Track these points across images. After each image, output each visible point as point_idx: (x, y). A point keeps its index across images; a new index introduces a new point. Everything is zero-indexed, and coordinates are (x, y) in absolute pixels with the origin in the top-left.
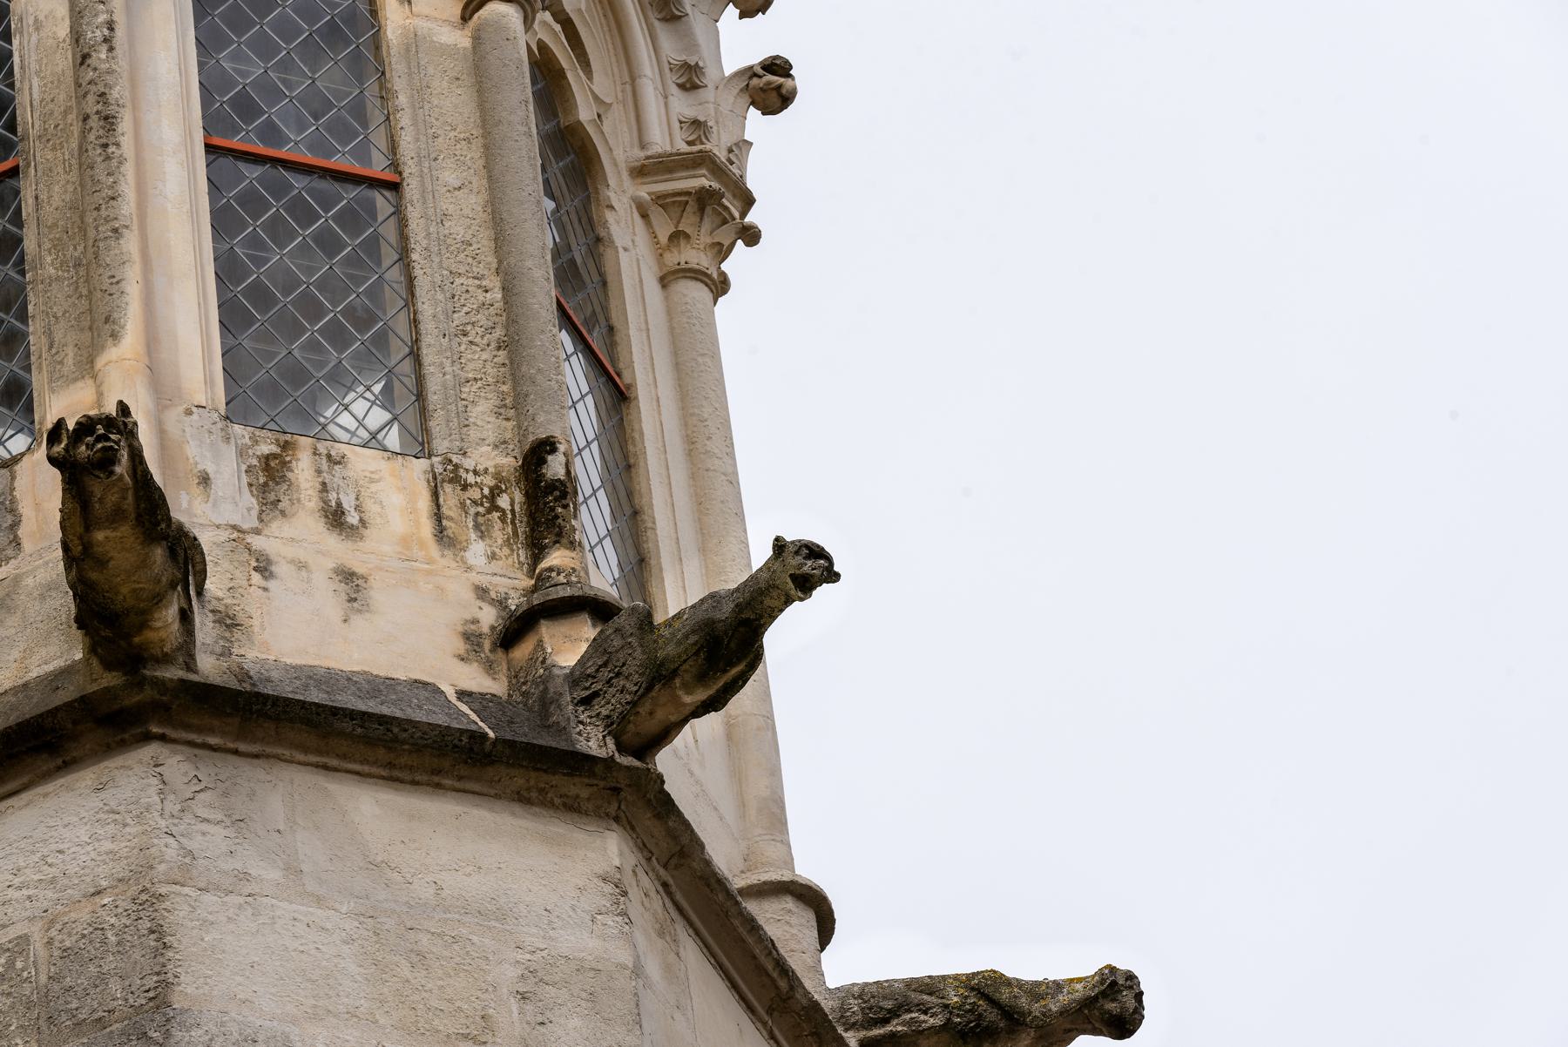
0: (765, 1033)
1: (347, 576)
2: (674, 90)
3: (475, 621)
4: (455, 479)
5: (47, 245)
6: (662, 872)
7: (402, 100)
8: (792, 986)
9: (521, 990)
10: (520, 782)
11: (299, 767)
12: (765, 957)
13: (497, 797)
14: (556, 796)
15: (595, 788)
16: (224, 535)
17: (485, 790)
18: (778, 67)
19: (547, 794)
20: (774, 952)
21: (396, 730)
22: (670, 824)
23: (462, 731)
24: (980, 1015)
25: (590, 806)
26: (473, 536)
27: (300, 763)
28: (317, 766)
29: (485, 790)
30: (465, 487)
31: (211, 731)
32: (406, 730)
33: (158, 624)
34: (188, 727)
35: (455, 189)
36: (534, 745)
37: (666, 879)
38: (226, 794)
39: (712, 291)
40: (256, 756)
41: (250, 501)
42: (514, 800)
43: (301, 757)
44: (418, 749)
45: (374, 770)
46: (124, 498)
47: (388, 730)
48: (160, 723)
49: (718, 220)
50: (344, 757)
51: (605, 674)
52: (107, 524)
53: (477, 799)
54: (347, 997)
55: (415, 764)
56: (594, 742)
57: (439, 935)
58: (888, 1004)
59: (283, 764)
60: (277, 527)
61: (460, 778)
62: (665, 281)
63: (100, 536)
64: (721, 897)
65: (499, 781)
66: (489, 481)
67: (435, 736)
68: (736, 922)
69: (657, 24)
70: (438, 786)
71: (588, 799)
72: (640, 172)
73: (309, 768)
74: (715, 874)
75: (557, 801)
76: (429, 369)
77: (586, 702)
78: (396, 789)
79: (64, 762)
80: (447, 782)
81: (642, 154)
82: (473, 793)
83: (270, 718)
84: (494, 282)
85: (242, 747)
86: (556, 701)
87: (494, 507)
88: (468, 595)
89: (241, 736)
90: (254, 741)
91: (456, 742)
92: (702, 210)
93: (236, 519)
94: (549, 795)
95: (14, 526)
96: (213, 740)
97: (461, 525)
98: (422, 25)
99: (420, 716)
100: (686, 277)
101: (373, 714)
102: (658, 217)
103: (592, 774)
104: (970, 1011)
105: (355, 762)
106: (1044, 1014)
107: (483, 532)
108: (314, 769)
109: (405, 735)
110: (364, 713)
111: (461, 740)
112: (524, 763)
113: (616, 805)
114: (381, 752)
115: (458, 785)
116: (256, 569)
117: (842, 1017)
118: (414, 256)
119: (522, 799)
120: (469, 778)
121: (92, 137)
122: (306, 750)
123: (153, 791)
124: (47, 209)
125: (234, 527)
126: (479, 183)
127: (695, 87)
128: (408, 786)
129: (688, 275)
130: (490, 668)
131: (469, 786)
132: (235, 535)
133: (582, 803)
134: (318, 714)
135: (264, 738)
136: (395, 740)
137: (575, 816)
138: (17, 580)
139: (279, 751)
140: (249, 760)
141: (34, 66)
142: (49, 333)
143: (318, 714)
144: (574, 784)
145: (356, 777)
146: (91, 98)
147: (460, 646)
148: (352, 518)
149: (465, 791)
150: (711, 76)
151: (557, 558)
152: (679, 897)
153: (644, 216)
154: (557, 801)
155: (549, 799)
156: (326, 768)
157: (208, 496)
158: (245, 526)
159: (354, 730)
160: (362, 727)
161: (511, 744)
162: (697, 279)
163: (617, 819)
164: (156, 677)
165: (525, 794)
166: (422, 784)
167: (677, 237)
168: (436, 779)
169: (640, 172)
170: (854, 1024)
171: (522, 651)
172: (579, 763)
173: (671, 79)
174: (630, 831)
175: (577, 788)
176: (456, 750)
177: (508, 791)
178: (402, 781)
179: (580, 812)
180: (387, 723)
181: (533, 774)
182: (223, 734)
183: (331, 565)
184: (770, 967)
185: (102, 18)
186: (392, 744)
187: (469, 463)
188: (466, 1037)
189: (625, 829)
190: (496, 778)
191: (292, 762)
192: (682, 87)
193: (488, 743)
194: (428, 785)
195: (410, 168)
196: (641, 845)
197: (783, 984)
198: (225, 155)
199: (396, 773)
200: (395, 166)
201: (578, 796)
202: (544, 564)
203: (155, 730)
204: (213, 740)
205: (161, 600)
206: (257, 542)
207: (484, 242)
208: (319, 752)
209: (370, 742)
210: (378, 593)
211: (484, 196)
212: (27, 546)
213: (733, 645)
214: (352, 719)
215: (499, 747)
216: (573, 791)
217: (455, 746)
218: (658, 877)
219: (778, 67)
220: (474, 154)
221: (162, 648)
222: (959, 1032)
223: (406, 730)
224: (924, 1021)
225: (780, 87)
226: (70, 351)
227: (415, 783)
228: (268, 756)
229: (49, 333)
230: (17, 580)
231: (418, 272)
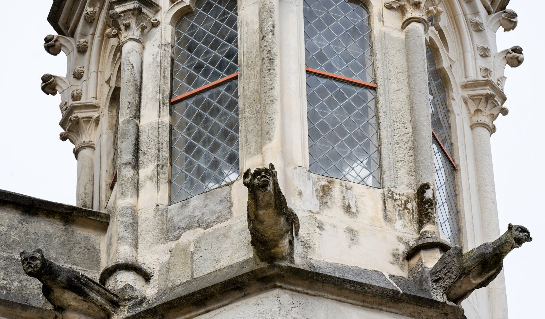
1: (351, 231)
2: (479, 57)
3: (397, 250)
4: (392, 197)
5: (247, 105)
7: (379, 57)
10: (411, 309)
11: (330, 300)
13: (402, 314)
15: (439, 313)
16: (307, 214)
17: (398, 312)
18: (517, 50)
19: (421, 314)
21: (366, 288)
23: (390, 290)
26: (398, 218)
27: (330, 299)
28: (337, 300)
29: (398, 312)
30: (395, 200)
31: (299, 285)
32: (370, 289)
33: (281, 246)
34: (290, 284)
35: (397, 90)
36: (417, 296)
38: (303, 309)
39: (489, 132)
40: (315, 296)
41: (317, 202)
42: (408, 316)
44: (374, 296)
45: (358, 303)
46: (271, 199)
47: (363, 288)
48: (280, 282)
49: (493, 106)
50: (347, 297)
51: (444, 271)
52: (264, 208)
53: (395, 315)
56: (439, 296)
59: (324, 299)
60: (326, 212)
61: (389, 307)
62: (472, 127)
63: (261, 212)
65: (403, 309)
66: (404, 198)
67: (381, 291)
69: (474, 33)
70: (381, 310)
71: (436, 317)
72: (465, 87)
73: (334, 301)
76: (384, 156)
77: (437, 281)
78: (365, 310)
79: (244, 294)
80: (384, 308)
81: (466, 80)
82: (394, 313)
83: (320, 282)
84: (409, 125)
85: (310, 292)
86: (425, 280)
87: (406, 208)
88: (395, 240)
89: (309, 288)
90: (314, 290)
92: (487, 102)
93: (311, 208)
94: (421, 315)
95: (230, 207)
96: (299, 289)
97: (393, 214)
98: (387, 30)
99: (375, 284)
100: (480, 126)
101: (358, 282)
102: (470, 102)
105: (351, 299)
107: (401, 217)
109: (369, 290)
110: (355, 282)
111: (390, 293)
112: (413, 303)
114: (360, 296)
115: (388, 309)
116: (317, 227)
118: (380, 114)
120: (392, 307)
121: (265, 66)
122: (333, 294)
123: (277, 306)
124: (248, 92)
125: (310, 211)
126: (406, 89)
127: (486, 56)
128: (370, 309)
129: (481, 125)
130: (402, 267)
132: (311, 214)
134: (338, 281)
135: (318, 289)
136: (366, 292)
138: (230, 227)
139: (323, 294)
140: (312, 297)
141: (245, 40)
142: (246, 137)
143: (338, 281)
144: (431, 311)
145: (351, 305)
146: (265, 52)
147: (391, 259)
148: (354, 210)
149: (391, 312)
150: (492, 53)
151: (428, 227)
153: (466, 103)
155: (421, 316)
156: (340, 301)
157: (301, 199)
158: (314, 211)
159: (351, 288)
160: (354, 287)
161: (408, 295)
162: (484, 127)
164: (280, 265)
166: (375, 309)
167: (477, 111)
168: (380, 307)
169: (465, 87)
171: (414, 261)
172: (433, 304)
173: (478, 53)
176: (388, 296)
177: (406, 313)
178: (368, 307)
180: (363, 286)
181: (416, 307)
182: (303, 287)
185: (271, 23)
186: (365, 293)
187: (397, 191)
190: (403, 308)
191: (328, 298)
192: (482, 56)
193: (400, 295)
194: (377, 309)
195: (380, 82)
199: (366, 304)
200: (375, 81)
201: (432, 316)
202: (423, 230)
203: (278, 284)
204: (299, 289)
205: (282, 237)
206: (318, 217)
207: (406, 110)
208: (338, 295)
209: (356, 292)
210: (362, 237)
211: (407, 93)
212: (235, 214)
214: (351, 284)
215: (404, 296)
217: (388, 295)
219: (517, 50)
220: (404, 78)
221: (282, 254)
223: (370, 289)
225: (518, 57)
226: (253, 144)
227: (372, 308)
228: (319, 296)
229: (246, 137)
230: (230, 227)
231: (381, 120)
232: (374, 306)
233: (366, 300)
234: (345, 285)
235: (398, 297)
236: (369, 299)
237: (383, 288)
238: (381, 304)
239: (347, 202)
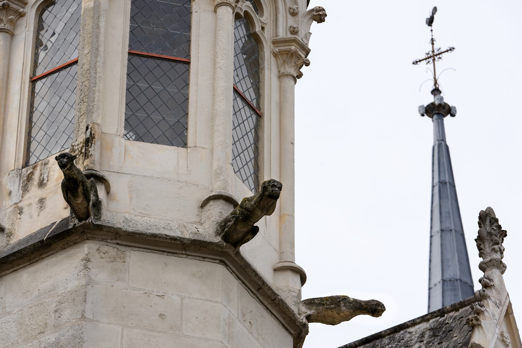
0: (185, 256)
6: (114, 241)
8: (181, 241)
9: (55, 310)
10: (61, 244)
12: (166, 240)
13: (57, 252)
14: (71, 243)
19: (68, 243)
20: (168, 237)
21: (23, 252)
22: (104, 230)
23: (38, 242)
24: (244, 213)
25: (80, 240)
27: (9, 273)
28: (13, 272)
29: (54, 252)
32: (25, 251)
35: (87, 54)
36: (55, 235)
37: (116, 242)
39: (228, 6)
42: (62, 250)
43: (8, 272)
44: (32, 253)
45: (26, 264)
47: (21, 253)
50: (19, 265)
54: (12, 339)
55: (35, 256)
57: (37, 305)
58: (223, 224)
60: (28, 195)
61: (47, 253)
64: (137, 236)
65: (56, 247)
67: (33, 247)
68: (149, 238)
70: (42, 258)
73: (11, 273)
74: (130, 232)
75: (72, 244)
78: (33, 266)
80: (44, 256)
82: (51, 255)
91: (38, 246)
100: (218, 7)
101: (16, 252)
103: (73, 233)
104: (242, 213)
105: (21, 264)
106: (251, 206)
108: (13, 273)
109: (26, 252)
110: (14, 253)
111: (39, 245)
112: (56, 241)
113: (86, 235)
115: (46, 255)
117: (217, 233)
119: (63, 249)
120: (49, 251)
122: (9, 269)
128: (36, 263)
129: (218, 6)
131: (49, 253)
132: (16, 205)
133: (77, 241)
137: (77, 245)
144: (73, 237)
145: (23, 269)
152: (124, 243)
154: (72, 244)
156: (15, 271)
157: (10, 198)
158: (18, 202)
159: (14, 258)
160: (15, 256)
162: (221, 6)
163: (88, 239)
165: (63, 247)
166: (35, 262)
168: (41, 257)
170: (220, 233)
174: (95, 239)
175: (74, 237)
179: (78, 243)
180: (20, 252)
181: (62, 241)
183: (37, 199)
184: (170, 241)
186: (25, 255)
188: (40, 333)
189: (92, 240)
190: (55, 247)
191: (7, 274)
193: (45, 242)
194: (40, 259)
196: (101, 240)
197: (178, 242)
198: (38, 81)
199: (32, 261)
201: (76, 239)
206: (20, 205)
208: (12, 267)
209: (21, 258)
213: (72, 185)
215: (48, 241)
216: (74, 238)
217: (38, 247)
218: (114, 243)
222: (242, 220)
223: (25, 251)
224: (230, 224)
227: (37, 261)
232: (37, 259)
233: (31, 258)
234: (10, 260)
235: (45, 244)
236: (32, 256)
237: (32, 244)
238: (41, 255)
239: (42, 177)
